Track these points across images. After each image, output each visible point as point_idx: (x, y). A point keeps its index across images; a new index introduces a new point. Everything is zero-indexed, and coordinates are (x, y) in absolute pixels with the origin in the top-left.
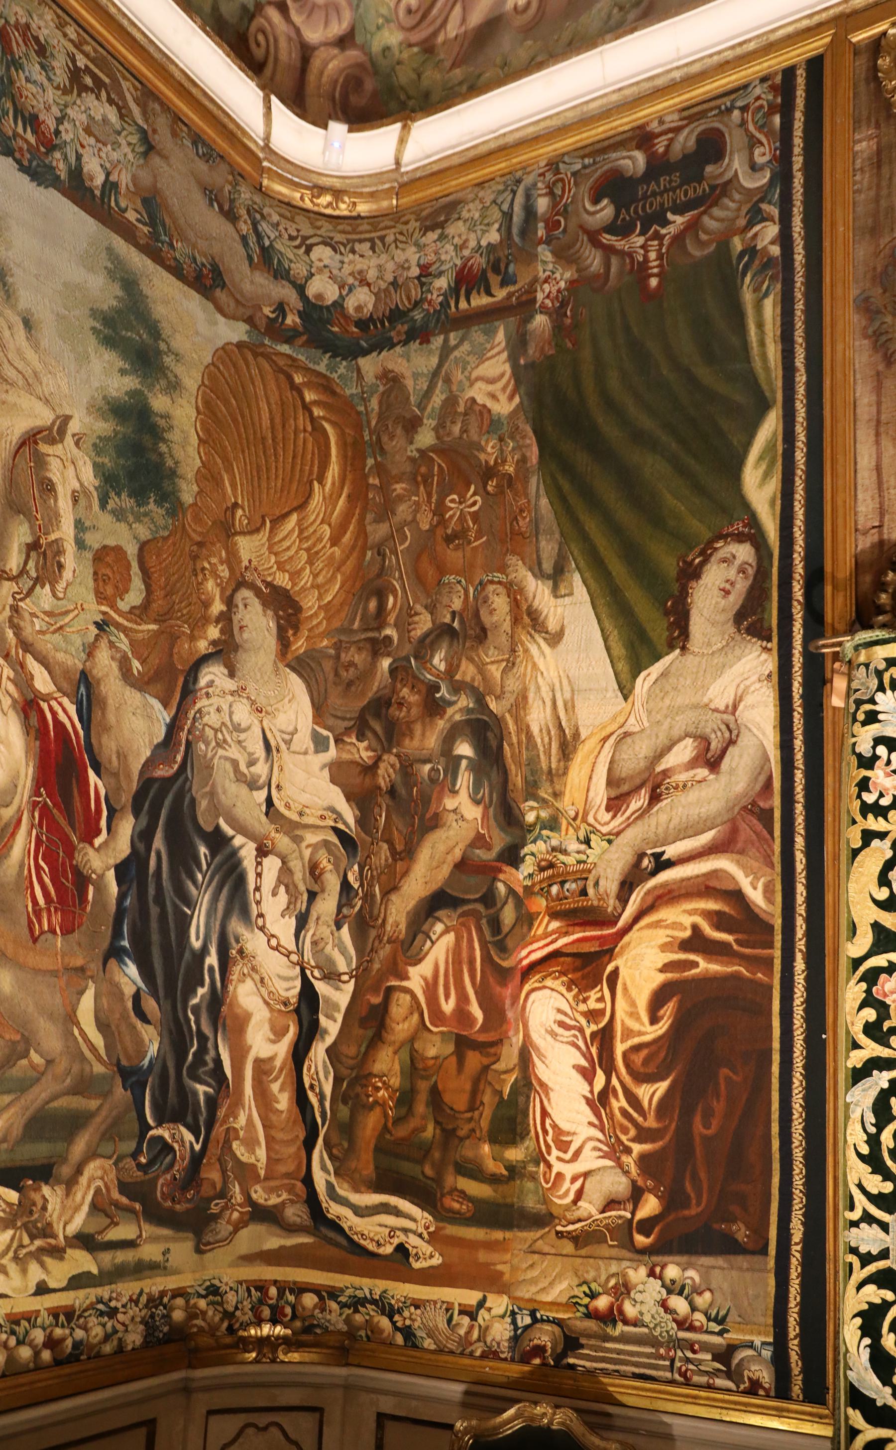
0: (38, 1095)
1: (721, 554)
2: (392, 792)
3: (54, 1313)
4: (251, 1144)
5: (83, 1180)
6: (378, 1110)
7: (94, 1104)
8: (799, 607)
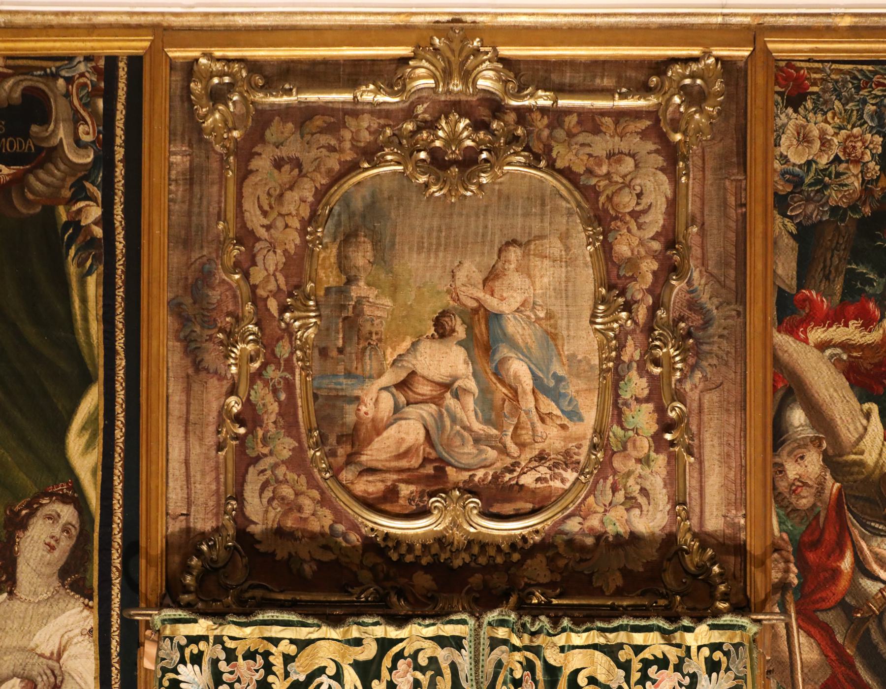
1: (47, 510)
8: (117, 573)
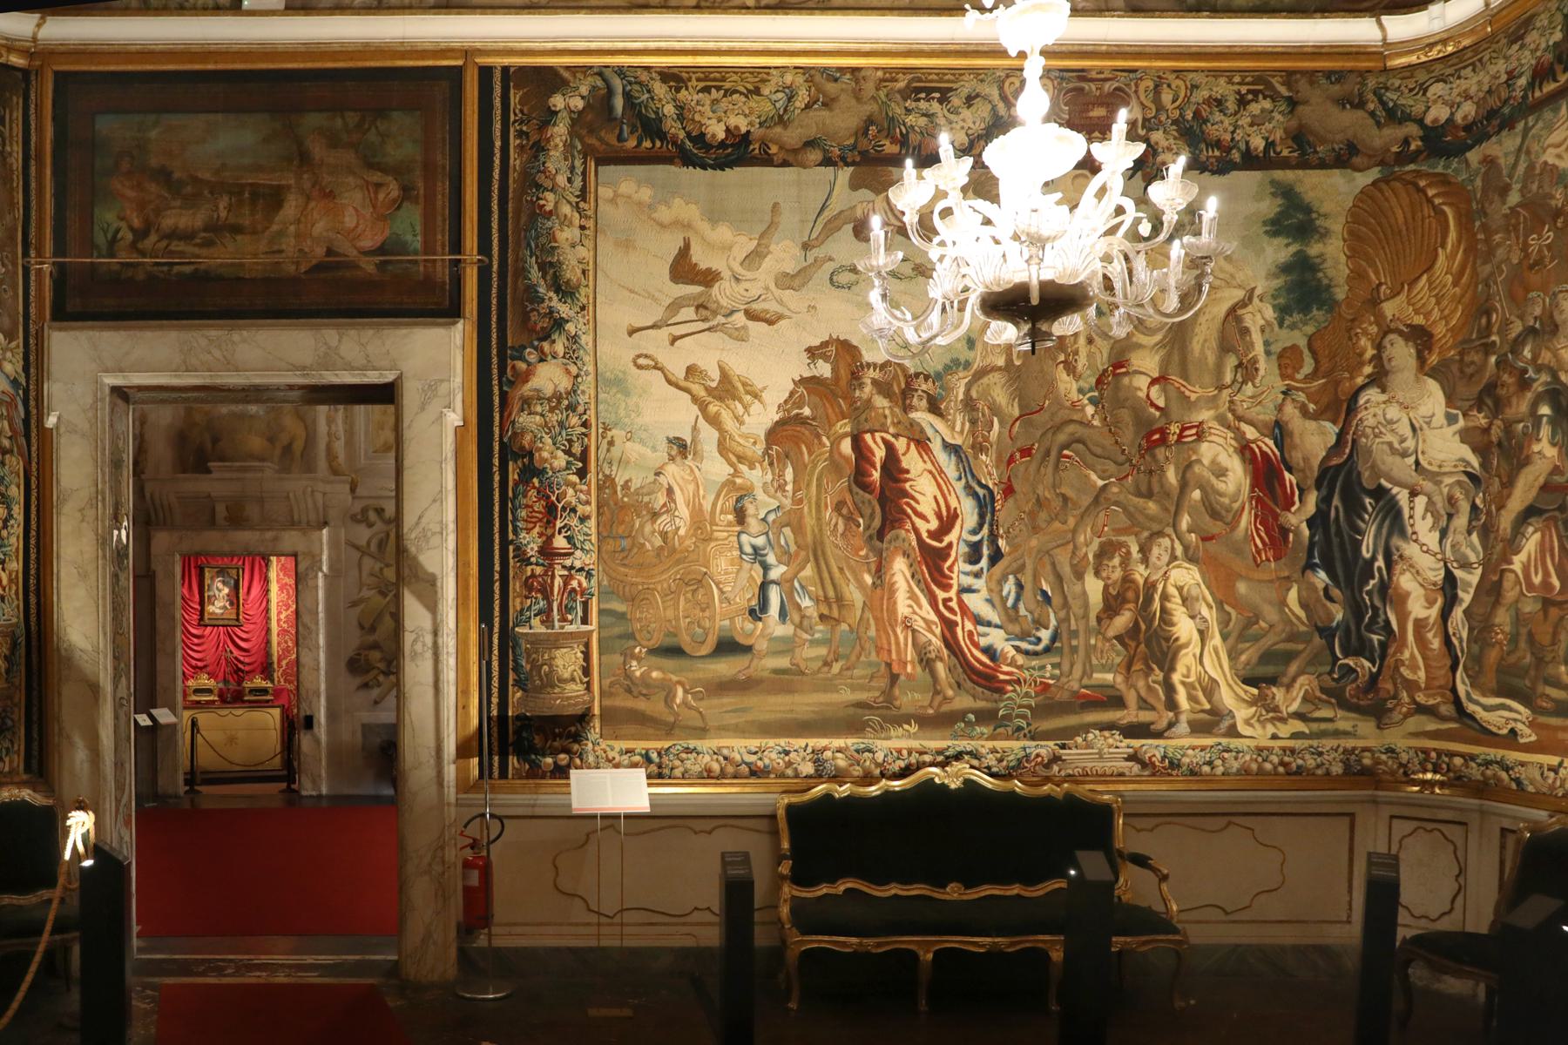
0: (1266, 643)
2: (1500, 444)
3: (1284, 749)
4: (1414, 668)
5: (1297, 685)
6: (1498, 647)
7: (1301, 647)
